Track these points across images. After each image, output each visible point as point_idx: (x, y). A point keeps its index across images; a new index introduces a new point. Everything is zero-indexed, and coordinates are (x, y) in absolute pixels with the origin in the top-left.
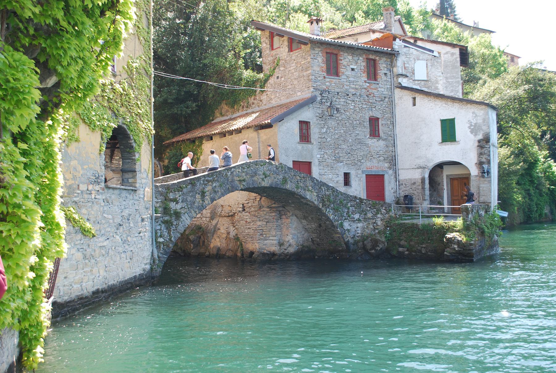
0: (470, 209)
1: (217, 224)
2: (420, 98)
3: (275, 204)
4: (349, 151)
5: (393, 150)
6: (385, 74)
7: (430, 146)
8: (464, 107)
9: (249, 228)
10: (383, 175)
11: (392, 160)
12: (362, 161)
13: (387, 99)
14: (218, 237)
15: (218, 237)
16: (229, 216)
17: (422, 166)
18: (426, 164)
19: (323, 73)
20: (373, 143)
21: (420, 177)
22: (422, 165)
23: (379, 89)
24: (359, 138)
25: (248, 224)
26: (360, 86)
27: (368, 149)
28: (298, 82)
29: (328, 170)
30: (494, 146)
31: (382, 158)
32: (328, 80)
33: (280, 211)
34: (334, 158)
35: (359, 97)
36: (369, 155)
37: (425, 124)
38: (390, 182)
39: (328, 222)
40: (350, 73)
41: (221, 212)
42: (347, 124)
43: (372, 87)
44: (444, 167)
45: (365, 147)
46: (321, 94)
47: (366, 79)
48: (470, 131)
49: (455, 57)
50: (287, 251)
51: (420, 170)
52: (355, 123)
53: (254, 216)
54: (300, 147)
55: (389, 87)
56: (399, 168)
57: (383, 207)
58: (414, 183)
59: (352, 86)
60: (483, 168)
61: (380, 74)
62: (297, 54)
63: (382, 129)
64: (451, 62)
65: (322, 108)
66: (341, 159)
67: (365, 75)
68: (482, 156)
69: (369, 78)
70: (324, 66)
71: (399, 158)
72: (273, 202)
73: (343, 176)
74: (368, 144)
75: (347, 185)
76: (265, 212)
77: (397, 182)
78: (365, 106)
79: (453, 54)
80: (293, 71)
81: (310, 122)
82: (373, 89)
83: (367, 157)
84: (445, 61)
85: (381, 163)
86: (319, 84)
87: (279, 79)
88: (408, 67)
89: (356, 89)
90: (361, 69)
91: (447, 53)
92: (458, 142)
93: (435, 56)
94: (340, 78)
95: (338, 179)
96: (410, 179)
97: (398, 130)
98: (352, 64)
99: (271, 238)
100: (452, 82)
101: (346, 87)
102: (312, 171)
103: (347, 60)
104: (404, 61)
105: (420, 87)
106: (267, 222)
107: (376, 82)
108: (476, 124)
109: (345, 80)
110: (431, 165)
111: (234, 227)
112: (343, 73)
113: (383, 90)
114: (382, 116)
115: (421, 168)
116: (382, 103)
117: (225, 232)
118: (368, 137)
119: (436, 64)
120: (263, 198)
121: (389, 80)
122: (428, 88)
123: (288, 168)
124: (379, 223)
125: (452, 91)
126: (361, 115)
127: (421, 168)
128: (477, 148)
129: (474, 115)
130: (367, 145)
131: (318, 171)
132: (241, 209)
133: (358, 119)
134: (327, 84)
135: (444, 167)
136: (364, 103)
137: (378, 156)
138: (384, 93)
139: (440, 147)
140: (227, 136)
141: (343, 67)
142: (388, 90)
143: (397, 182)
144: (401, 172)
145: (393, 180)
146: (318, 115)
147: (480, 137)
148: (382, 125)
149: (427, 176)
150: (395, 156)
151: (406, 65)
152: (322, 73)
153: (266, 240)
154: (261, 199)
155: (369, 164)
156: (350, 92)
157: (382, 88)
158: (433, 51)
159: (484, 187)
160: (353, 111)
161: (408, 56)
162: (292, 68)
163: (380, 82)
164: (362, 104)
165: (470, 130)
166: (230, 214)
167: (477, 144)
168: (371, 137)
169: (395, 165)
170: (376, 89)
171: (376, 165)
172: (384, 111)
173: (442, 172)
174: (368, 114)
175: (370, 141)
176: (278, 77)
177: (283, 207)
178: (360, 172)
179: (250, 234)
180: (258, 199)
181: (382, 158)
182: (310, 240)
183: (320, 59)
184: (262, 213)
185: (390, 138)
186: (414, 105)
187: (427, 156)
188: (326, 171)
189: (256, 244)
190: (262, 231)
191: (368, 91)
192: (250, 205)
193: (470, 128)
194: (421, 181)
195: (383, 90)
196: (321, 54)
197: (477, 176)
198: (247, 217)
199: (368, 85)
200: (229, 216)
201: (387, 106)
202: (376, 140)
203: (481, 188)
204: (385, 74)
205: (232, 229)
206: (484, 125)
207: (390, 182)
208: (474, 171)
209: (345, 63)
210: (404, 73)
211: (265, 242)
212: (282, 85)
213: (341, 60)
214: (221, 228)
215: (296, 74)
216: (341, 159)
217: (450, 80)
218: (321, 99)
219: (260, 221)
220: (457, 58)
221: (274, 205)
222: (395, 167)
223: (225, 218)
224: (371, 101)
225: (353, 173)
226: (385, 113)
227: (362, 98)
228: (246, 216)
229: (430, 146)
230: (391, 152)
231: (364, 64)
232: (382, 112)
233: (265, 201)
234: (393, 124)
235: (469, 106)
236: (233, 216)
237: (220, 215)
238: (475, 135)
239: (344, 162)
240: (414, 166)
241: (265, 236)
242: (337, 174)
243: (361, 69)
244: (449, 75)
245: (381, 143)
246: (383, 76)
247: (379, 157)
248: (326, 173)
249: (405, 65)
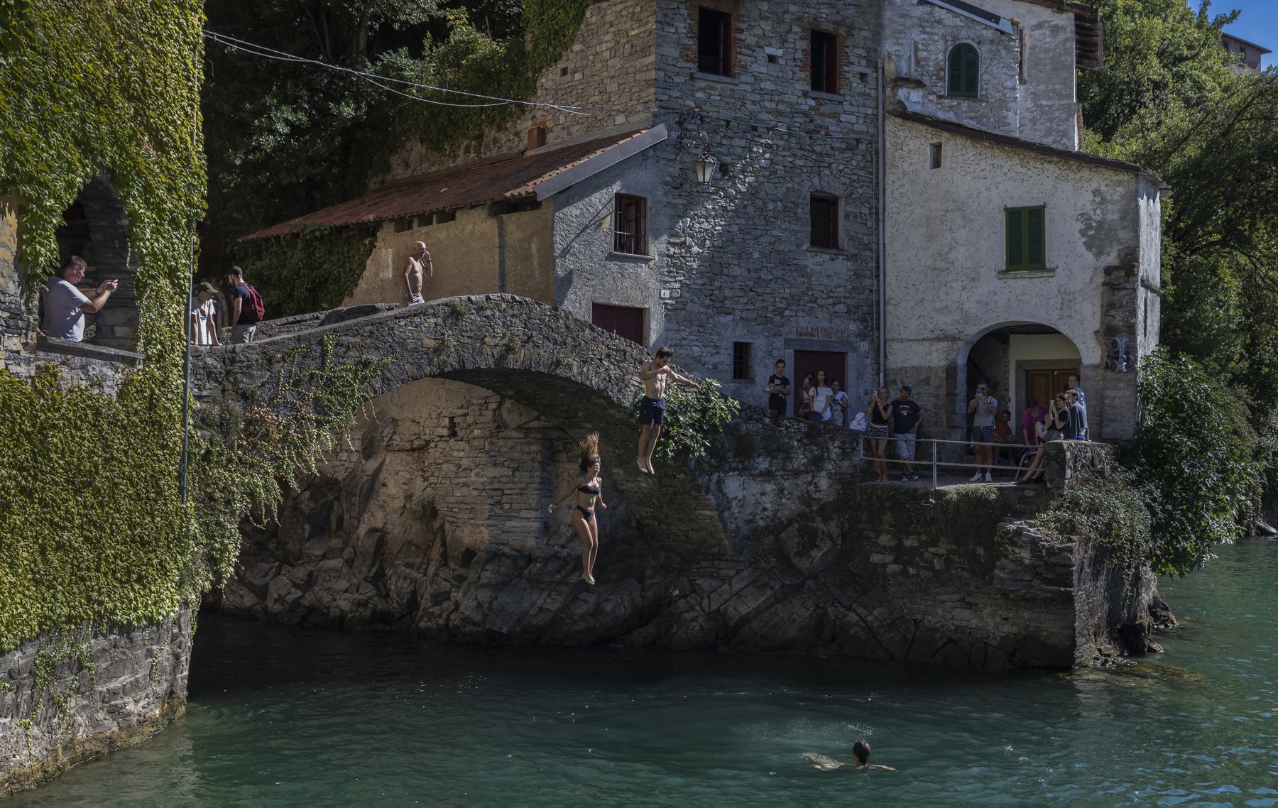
0: (1068, 454)
1: (378, 471)
2: (953, 147)
3: (538, 419)
4: (750, 283)
5: (874, 288)
6: (863, 76)
7: (973, 279)
8: (1071, 176)
9: (465, 485)
10: (842, 356)
11: (870, 314)
12: (787, 313)
13: (862, 147)
14: (381, 506)
15: (381, 506)
16: (413, 450)
17: (948, 333)
18: (960, 327)
19: (689, 65)
20: (817, 262)
21: (944, 363)
22: (952, 330)
23: (844, 118)
24: (781, 248)
25: (463, 474)
26: (790, 104)
27: (806, 280)
28: (619, 85)
29: (691, 333)
30: (1148, 287)
31: (841, 308)
32: (702, 84)
33: (551, 441)
34: (707, 302)
35: (786, 137)
36: (806, 298)
37: (963, 218)
38: (860, 376)
39: (682, 475)
40: (763, 70)
41: (391, 439)
42: (751, 209)
43: (822, 109)
44: (1012, 337)
45: (795, 274)
46: (680, 123)
47: (808, 88)
48: (1085, 243)
49: (1062, 36)
51: (943, 345)
52: (771, 207)
53: (482, 450)
55: (870, 111)
56: (888, 336)
57: (834, 441)
58: (927, 381)
59: (768, 104)
60: (1115, 344)
61: (847, 75)
62: (619, 8)
63: (844, 227)
64: (1047, 51)
65: (681, 162)
66: (728, 304)
67: (804, 75)
68: (1113, 312)
69: (816, 85)
70: (692, 43)
71: (889, 308)
72: (535, 414)
73: (731, 352)
74: (806, 267)
75: (741, 377)
76: (510, 442)
77: (882, 375)
78: (800, 163)
79: (1056, 30)
80: (607, 55)
81: (645, 199)
82: (825, 115)
83: (801, 302)
84: (1033, 48)
85: (838, 321)
86: (677, 94)
87: (568, 77)
88: (926, 59)
89: (779, 113)
90: (795, 60)
91: (1040, 25)
92: (1053, 270)
93: (1002, 33)
94: (737, 81)
95: (716, 359)
96: (917, 369)
97: (889, 232)
98: (770, 45)
99: (523, 514)
100: (1051, 107)
101: (750, 106)
102: (645, 334)
103: (758, 31)
104: (916, 43)
106: (515, 470)
107: (836, 97)
108: (1101, 223)
109: (749, 88)
110: (973, 331)
111: (425, 479)
112: (745, 67)
113: (853, 119)
114: (847, 193)
115: (946, 338)
116: (848, 155)
117: (401, 494)
118: (804, 247)
119: (1003, 53)
120: (508, 403)
121: (873, 93)
122: (979, 121)
123: (576, 320)
124: (824, 483)
125: (1048, 132)
126: (790, 185)
127: (946, 338)
128: (1101, 289)
129: (1098, 199)
130: (803, 270)
132: (445, 432)
133: (780, 195)
134: (699, 95)
135: (1012, 337)
136: (800, 153)
137: (831, 301)
138: (857, 128)
139: (1001, 283)
140: (415, 225)
141: (744, 51)
142: (868, 121)
143: (882, 375)
144: (894, 347)
145: (869, 371)
146: (669, 179)
147: (1112, 258)
148: (847, 216)
149: (962, 361)
151: (923, 54)
152: (684, 64)
153: (510, 518)
154: (500, 404)
155: (804, 322)
156: (762, 121)
157: (852, 113)
158: (997, 19)
159: (1115, 398)
160: (767, 173)
161: (928, 30)
162: (604, 46)
163: (848, 98)
164: (794, 155)
165: (1084, 239)
166: (417, 443)
167: (1101, 278)
168: (814, 249)
169: (878, 329)
170: (835, 115)
171: (826, 325)
172: (855, 177)
173: (1005, 352)
174: (809, 184)
175: (811, 260)
176: (564, 72)
177: (562, 429)
178: (779, 342)
179: (467, 500)
180: (493, 406)
181: (841, 308)
182: (634, 524)
183: (681, 26)
184: (501, 442)
185: (868, 253)
186: (937, 163)
187: (965, 307)
188: (684, 334)
189: (483, 529)
190: (500, 493)
191: (812, 121)
192: (470, 419)
193: (1083, 235)
194: (944, 375)
195: (853, 119)
196: (685, 12)
197: (1096, 367)
198: (462, 454)
199: (813, 103)
200: (413, 450)
201: (862, 164)
202: (827, 257)
203: (1107, 401)
204: (863, 76)
205: (419, 484)
206: (1124, 228)
207: (860, 376)
208: (1091, 354)
209: (751, 40)
210: (914, 75)
211: (509, 524)
212: (575, 92)
213: (741, 31)
214: (391, 483)
215: (615, 63)
216: (728, 304)
217: (1044, 102)
218: (679, 137)
219: (495, 465)
220: (1066, 40)
221: (535, 424)
222: (876, 334)
223: (403, 455)
224: (817, 148)
225: (759, 344)
226: (855, 185)
227: (793, 140)
228: (459, 450)
229: (973, 279)
230: (867, 292)
231: (804, 45)
232: (848, 182)
233: (513, 415)
234: (877, 214)
235: (1085, 173)
236: (423, 448)
237: (388, 446)
238: (1098, 255)
239: (738, 313)
240: (927, 334)
241: (507, 507)
242: (716, 347)
243: (795, 60)
244: (1042, 87)
245: (841, 267)
246: (856, 82)
247: (834, 304)
248: (684, 343)
249: (919, 53)
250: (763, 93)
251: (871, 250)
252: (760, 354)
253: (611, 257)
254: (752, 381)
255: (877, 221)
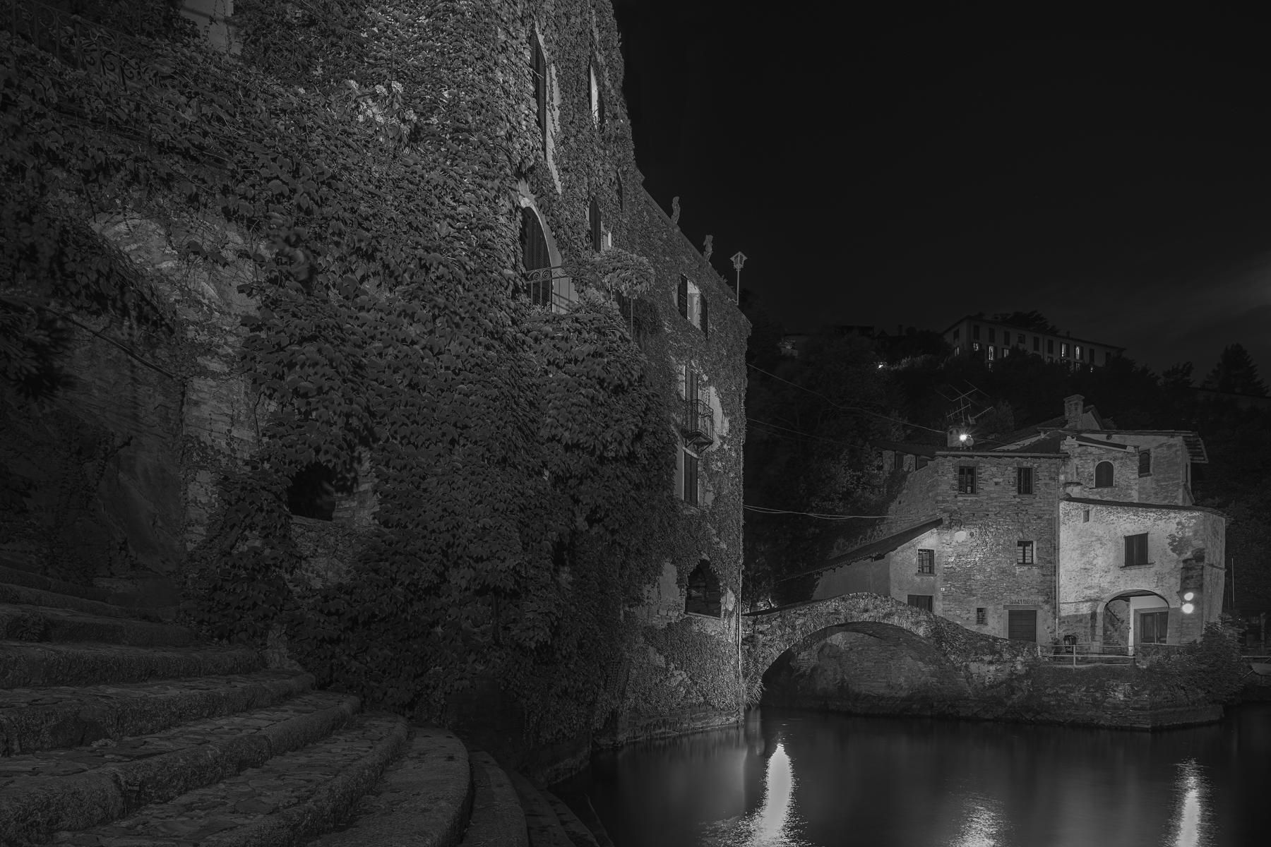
23: (1036, 505)
32: (961, 499)
47: (1017, 494)
50: (897, 696)
54: (918, 579)
58: (1081, 621)
105: (1101, 496)
116: (1039, 521)
119: (1129, 463)
131: (942, 606)
150: (1055, 587)
195: (1042, 505)
240: (1080, 599)
250: (992, 499)
251: (1051, 563)
252: (990, 612)
253: (916, 574)
254: (986, 624)
255: (1055, 549)
